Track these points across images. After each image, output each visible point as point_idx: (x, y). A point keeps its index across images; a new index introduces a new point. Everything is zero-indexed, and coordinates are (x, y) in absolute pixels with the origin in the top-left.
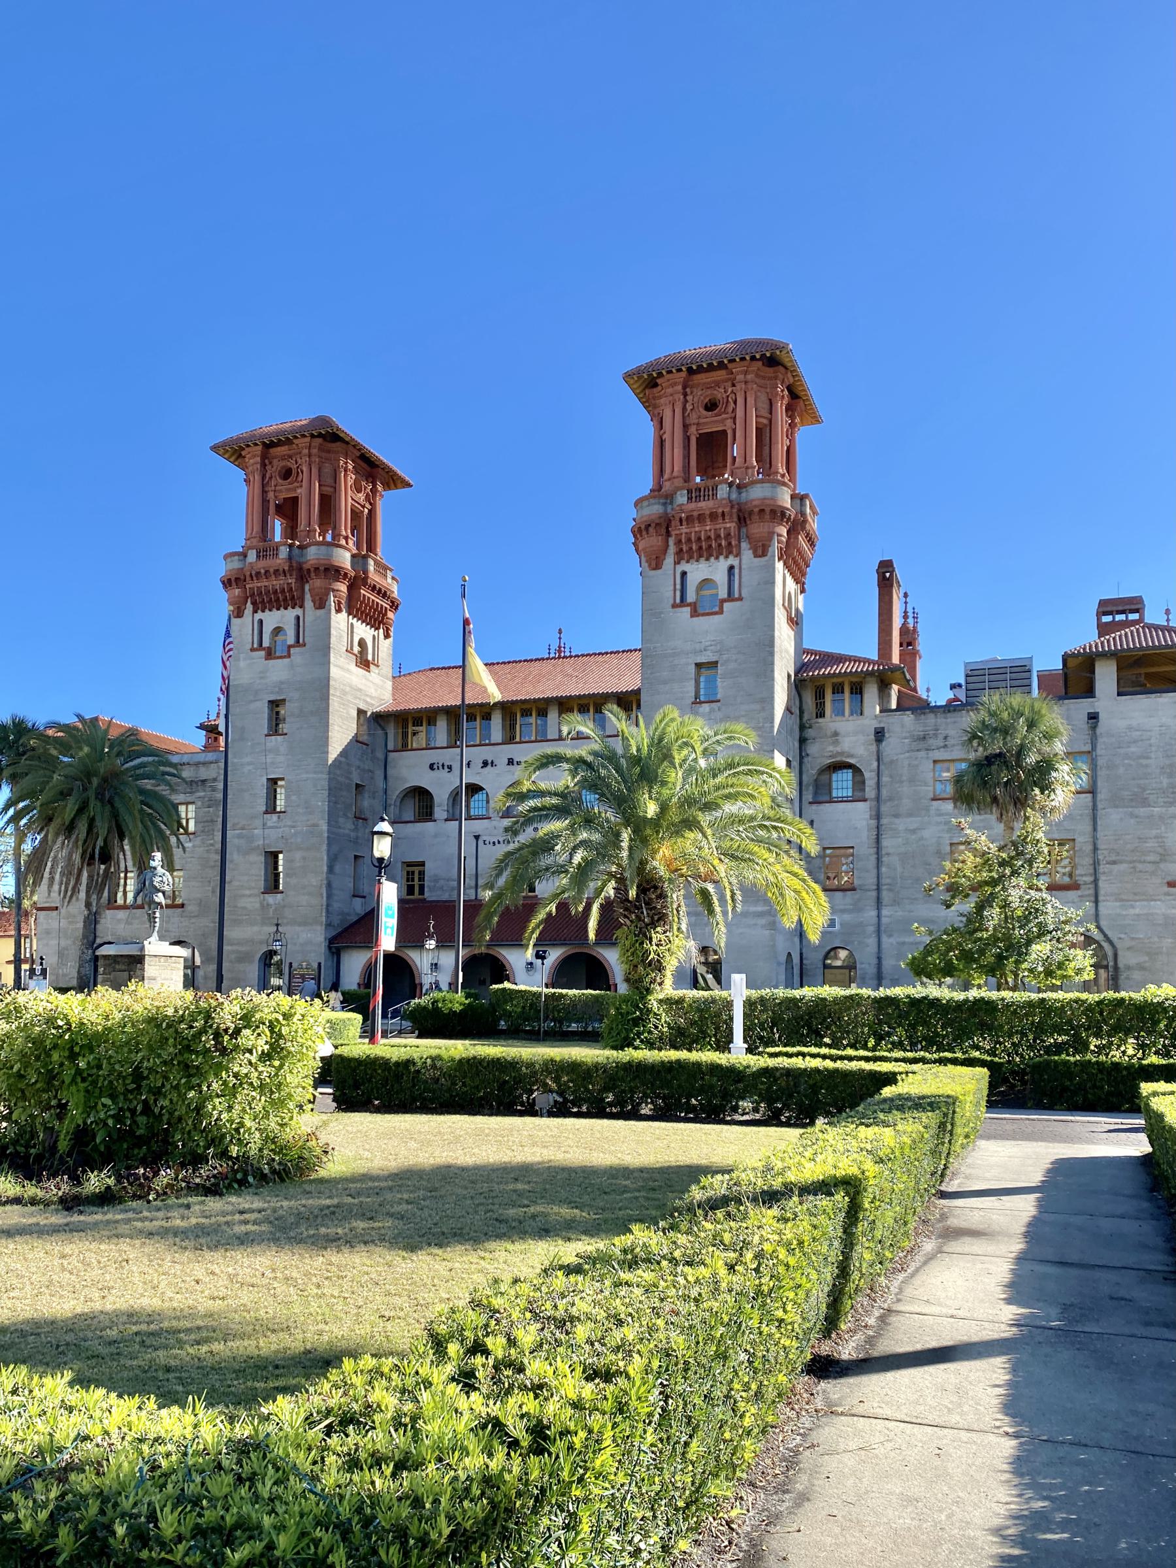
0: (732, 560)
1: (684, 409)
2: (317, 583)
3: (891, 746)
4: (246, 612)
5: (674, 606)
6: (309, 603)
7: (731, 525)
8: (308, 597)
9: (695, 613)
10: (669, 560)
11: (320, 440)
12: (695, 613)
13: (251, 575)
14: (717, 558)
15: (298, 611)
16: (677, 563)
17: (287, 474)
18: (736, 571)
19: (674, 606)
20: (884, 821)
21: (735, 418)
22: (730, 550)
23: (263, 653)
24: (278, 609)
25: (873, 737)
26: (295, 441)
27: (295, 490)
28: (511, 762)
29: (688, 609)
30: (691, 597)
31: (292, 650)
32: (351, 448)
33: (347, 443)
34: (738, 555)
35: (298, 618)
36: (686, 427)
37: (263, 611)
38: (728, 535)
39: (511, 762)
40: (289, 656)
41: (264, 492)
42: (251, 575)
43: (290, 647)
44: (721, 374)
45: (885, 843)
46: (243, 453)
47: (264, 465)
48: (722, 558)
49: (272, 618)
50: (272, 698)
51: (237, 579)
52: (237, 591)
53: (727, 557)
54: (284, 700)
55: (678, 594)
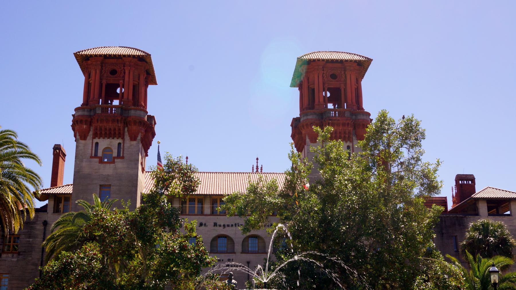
1: (323, 77)
2: (134, 128)
4: (88, 138)
6: (127, 137)
7: (351, 129)
8: (126, 134)
11: (136, 60)
15: (120, 141)
17: (113, 72)
21: (345, 84)
23: (97, 160)
24: (109, 138)
26: (123, 58)
28: (215, 225)
31: (116, 160)
33: (147, 62)
34: (352, 141)
35: (119, 144)
36: (324, 84)
37: (99, 138)
38: (349, 133)
39: (215, 225)
40: (114, 162)
41: (101, 79)
43: (114, 158)
44: (339, 65)
47: (102, 66)
49: (104, 143)
50: (102, 183)
52: (85, 126)
53: (346, 142)
54: (110, 185)
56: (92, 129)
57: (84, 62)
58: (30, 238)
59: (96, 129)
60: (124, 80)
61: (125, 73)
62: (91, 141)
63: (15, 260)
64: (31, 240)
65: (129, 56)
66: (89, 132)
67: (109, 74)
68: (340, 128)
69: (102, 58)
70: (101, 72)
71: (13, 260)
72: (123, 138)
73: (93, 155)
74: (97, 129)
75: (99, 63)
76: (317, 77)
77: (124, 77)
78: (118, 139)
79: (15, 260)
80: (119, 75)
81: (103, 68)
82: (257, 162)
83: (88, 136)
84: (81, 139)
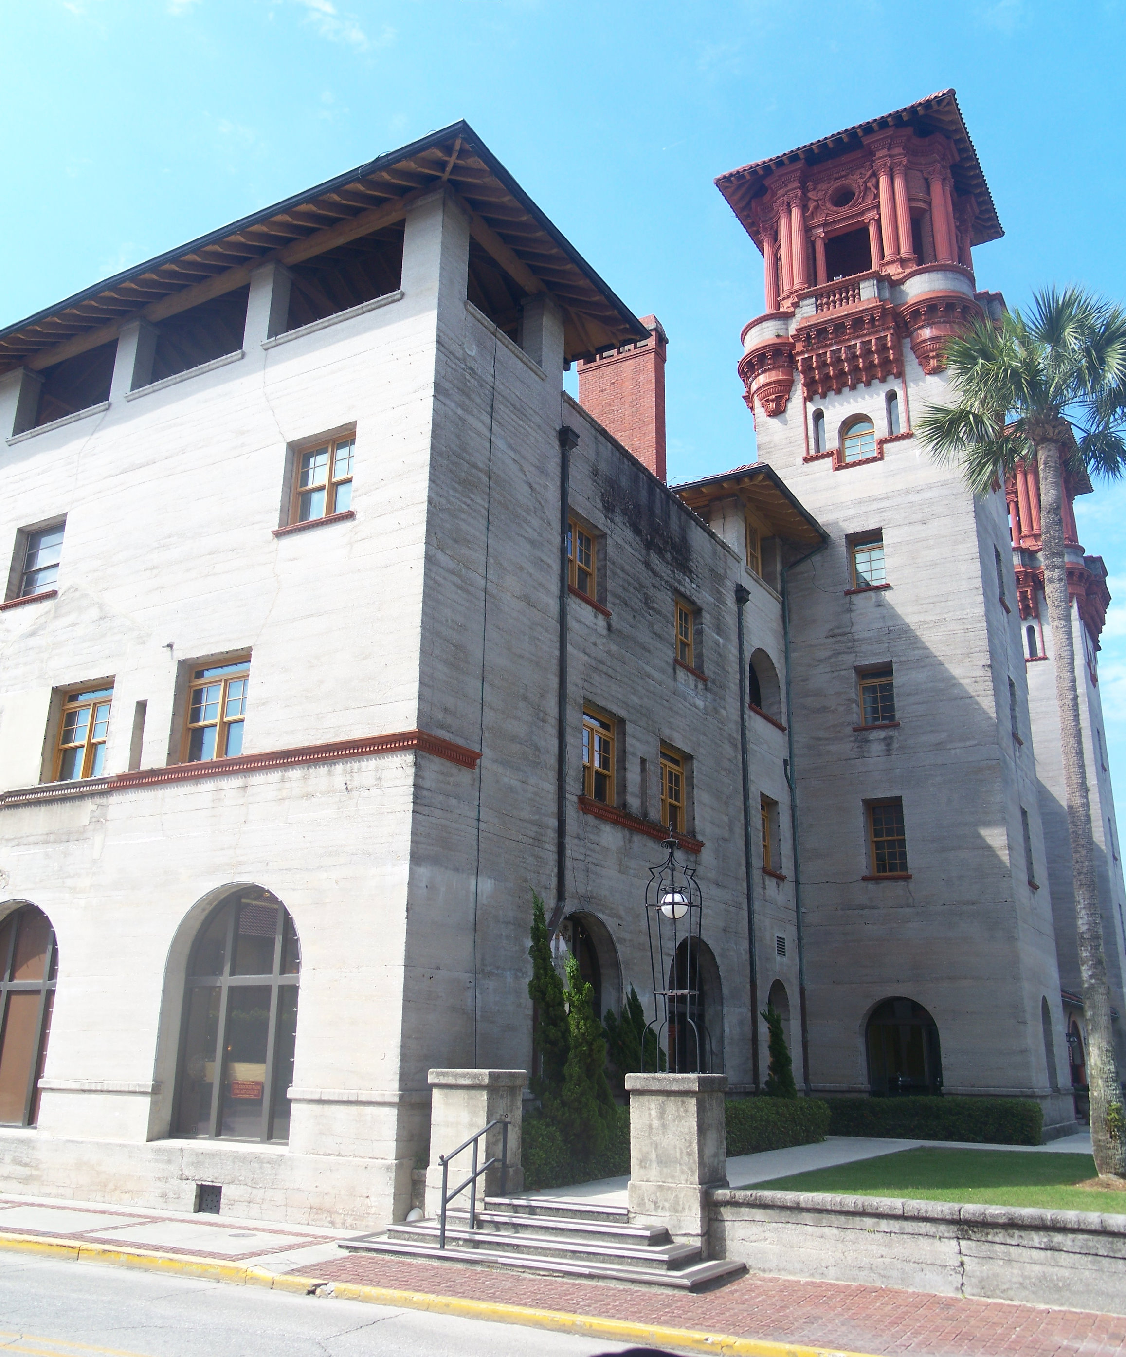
11: (909, 130)
17: (843, 197)
27: (863, 213)
32: (953, 145)
37: (824, 396)
43: (882, 442)
46: (767, 182)
57: (753, 205)
59: (808, 369)
61: (877, 187)
65: (882, 123)
67: (829, 205)
69: (800, 165)
70: (804, 208)
72: (900, 375)
73: (812, 452)
74: (811, 369)
75: (796, 184)
77: (877, 196)
78: (883, 380)
80: (860, 200)
81: (810, 195)
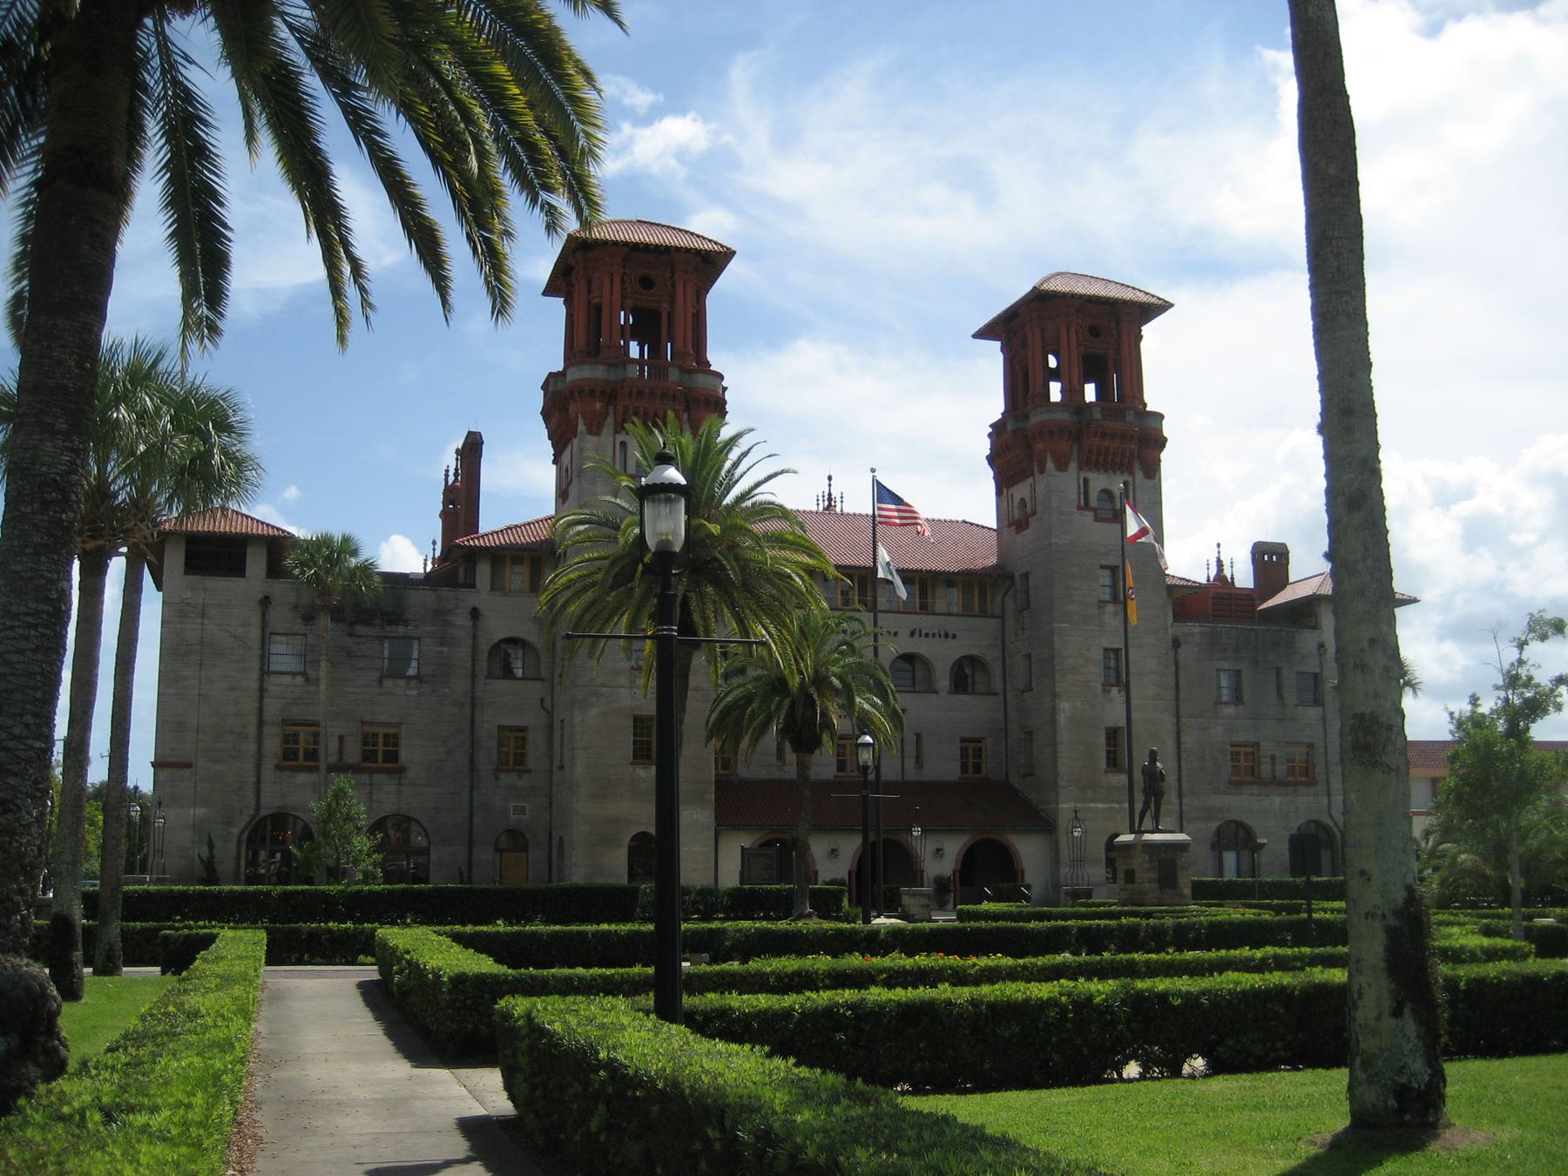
0: (1126, 477)
3: (1184, 651)
5: (1079, 508)
9: (1097, 519)
10: (1073, 466)
11: (699, 259)
12: (1097, 519)
13: (630, 394)
14: (1114, 472)
16: (1080, 468)
18: (1131, 487)
19: (1079, 508)
20: (1183, 720)
22: (1129, 469)
25: (1170, 644)
29: (1092, 513)
30: (1093, 501)
34: (1131, 473)
41: (623, 297)
42: (630, 394)
45: (1184, 738)
48: (1118, 473)
51: (603, 392)
52: (598, 406)
53: (1122, 473)
55: (1082, 497)
56: (611, 411)
58: (442, 645)
60: (673, 302)
61: (673, 286)
62: (611, 439)
63: (414, 692)
64: (446, 649)
66: (606, 417)
68: (1116, 445)
70: (623, 283)
71: (408, 692)
76: (1065, 331)
79: (414, 692)
82: (830, 485)
83: (603, 426)
84: (590, 432)
